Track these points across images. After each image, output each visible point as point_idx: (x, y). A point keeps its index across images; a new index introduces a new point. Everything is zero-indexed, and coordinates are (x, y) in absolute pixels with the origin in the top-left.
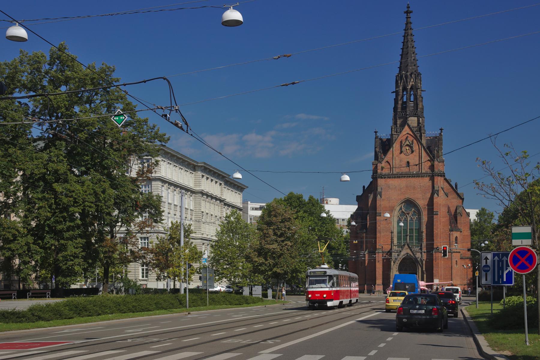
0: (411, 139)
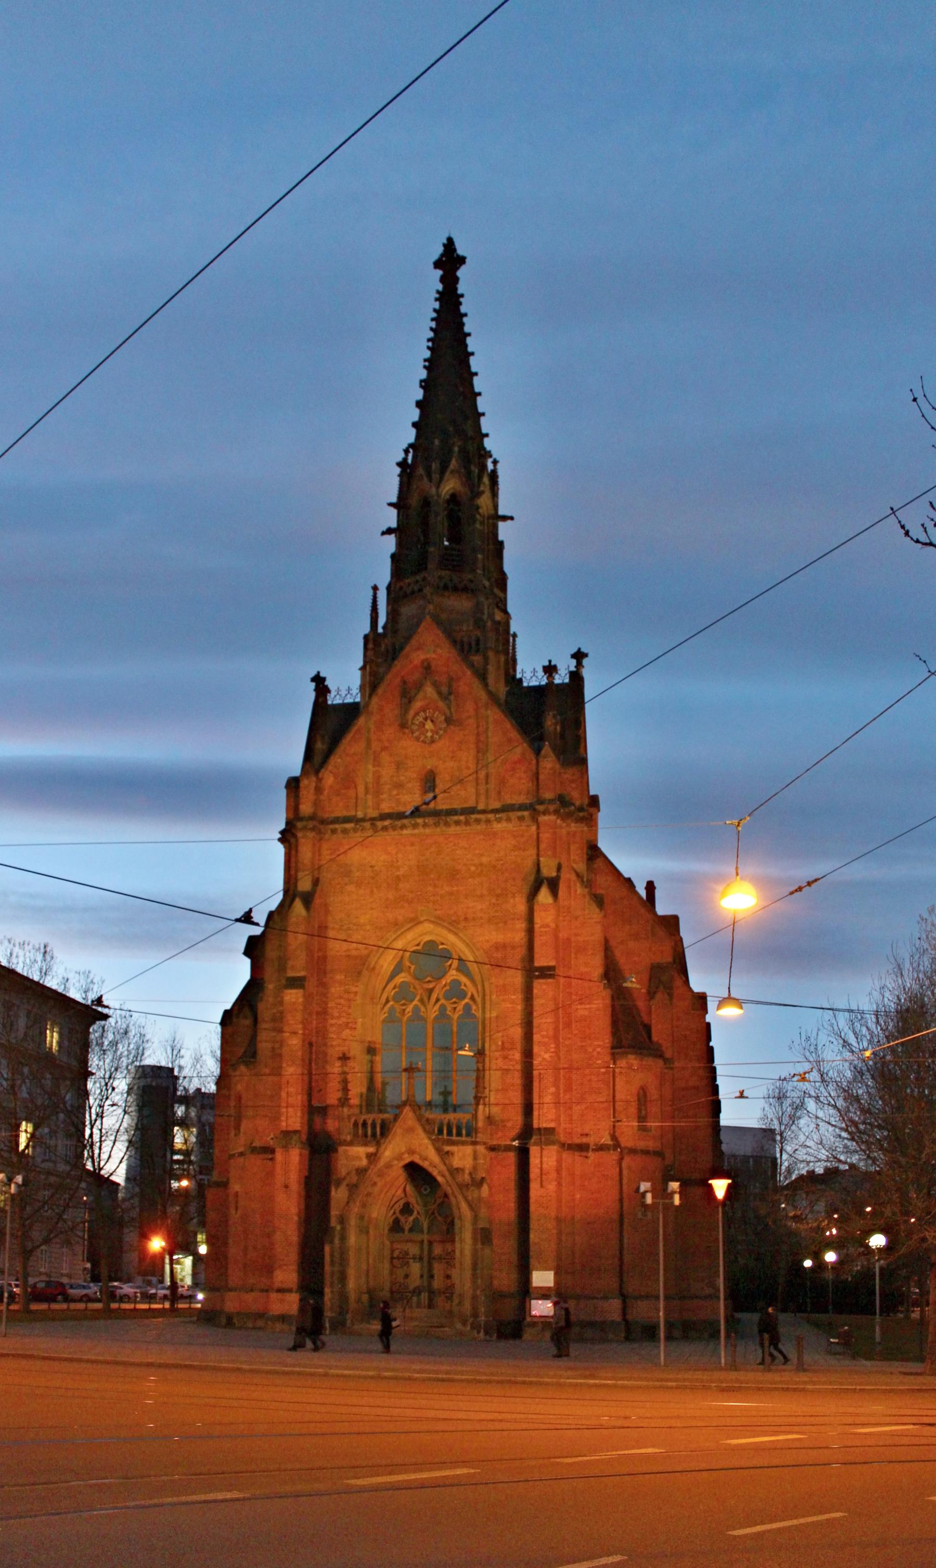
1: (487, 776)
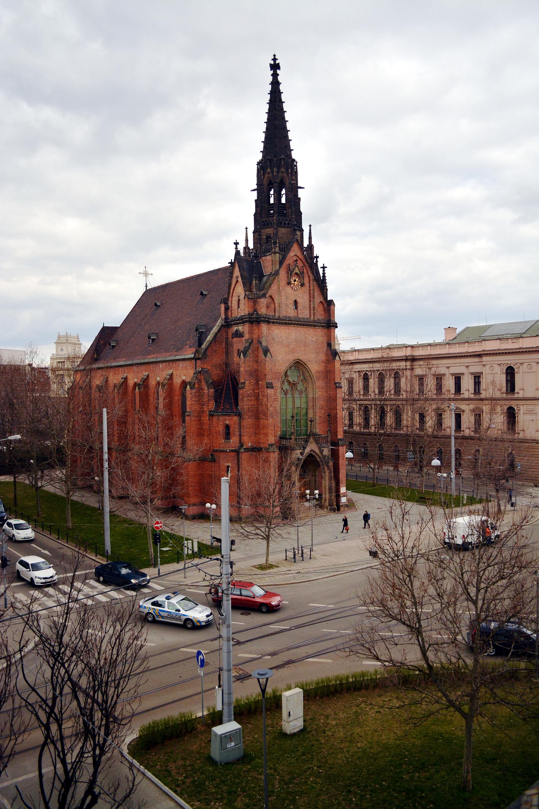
0: (300, 264)
1: (314, 308)
